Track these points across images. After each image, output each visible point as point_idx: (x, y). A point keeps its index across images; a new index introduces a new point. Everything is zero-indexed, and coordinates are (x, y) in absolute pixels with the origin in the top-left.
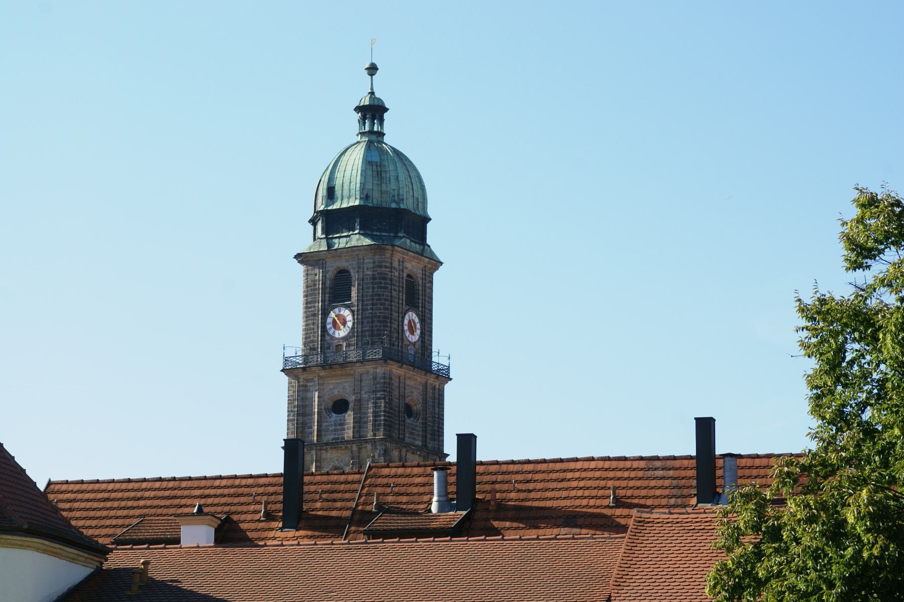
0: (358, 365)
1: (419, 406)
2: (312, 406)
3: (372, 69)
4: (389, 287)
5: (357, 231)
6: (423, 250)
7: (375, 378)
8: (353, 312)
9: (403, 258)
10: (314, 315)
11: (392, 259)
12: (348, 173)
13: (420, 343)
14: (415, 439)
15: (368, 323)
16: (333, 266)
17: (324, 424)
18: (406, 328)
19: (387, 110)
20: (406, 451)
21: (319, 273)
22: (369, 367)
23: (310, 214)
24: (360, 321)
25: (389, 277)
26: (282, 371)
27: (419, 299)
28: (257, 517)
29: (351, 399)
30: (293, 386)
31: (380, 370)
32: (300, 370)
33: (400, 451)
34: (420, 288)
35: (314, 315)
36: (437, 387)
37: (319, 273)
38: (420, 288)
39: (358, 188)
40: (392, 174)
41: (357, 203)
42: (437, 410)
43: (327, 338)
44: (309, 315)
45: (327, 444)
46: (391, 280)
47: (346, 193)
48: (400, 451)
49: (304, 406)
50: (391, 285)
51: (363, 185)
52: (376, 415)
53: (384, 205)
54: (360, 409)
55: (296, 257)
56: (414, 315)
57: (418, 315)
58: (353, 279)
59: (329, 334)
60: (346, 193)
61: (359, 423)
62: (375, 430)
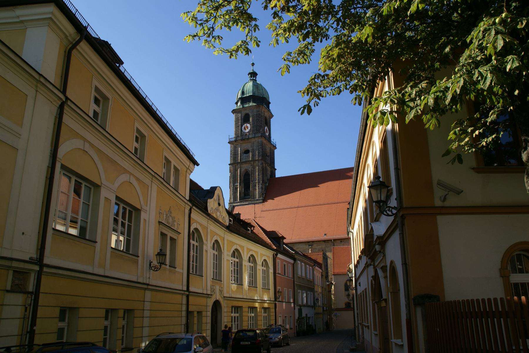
2: (238, 152)
3: (253, 64)
7: (258, 142)
8: (251, 125)
10: (238, 127)
12: (248, 88)
16: (244, 113)
17: (242, 157)
21: (240, 115)
22: (256, 139)
24: (253, 127)
26: (229, 143)
29: (250, 149)
31: (260, 140)
37: (240, 115)
39: (252, 90)
40: (261, 88)
41: (251, 94)
43: (243, 132)
44: (237, 126)
45: (243, 162)
47: (248, 92)
49: (236, 152)
51: (253, 90)
52: (259, 153)
54: (253, 152)
58: (250, 115)
60: (248, 92)
61: (253, 156)
62: (259, 156)
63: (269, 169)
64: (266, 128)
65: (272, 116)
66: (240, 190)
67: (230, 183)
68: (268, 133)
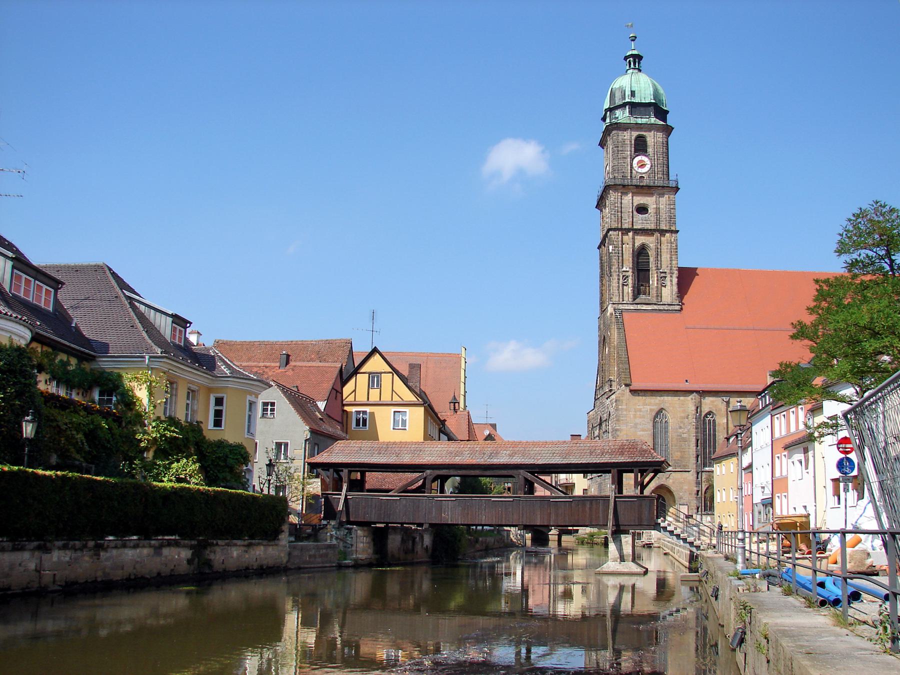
0: (660, 188)
43: (633, 171)
59: (635, 170)
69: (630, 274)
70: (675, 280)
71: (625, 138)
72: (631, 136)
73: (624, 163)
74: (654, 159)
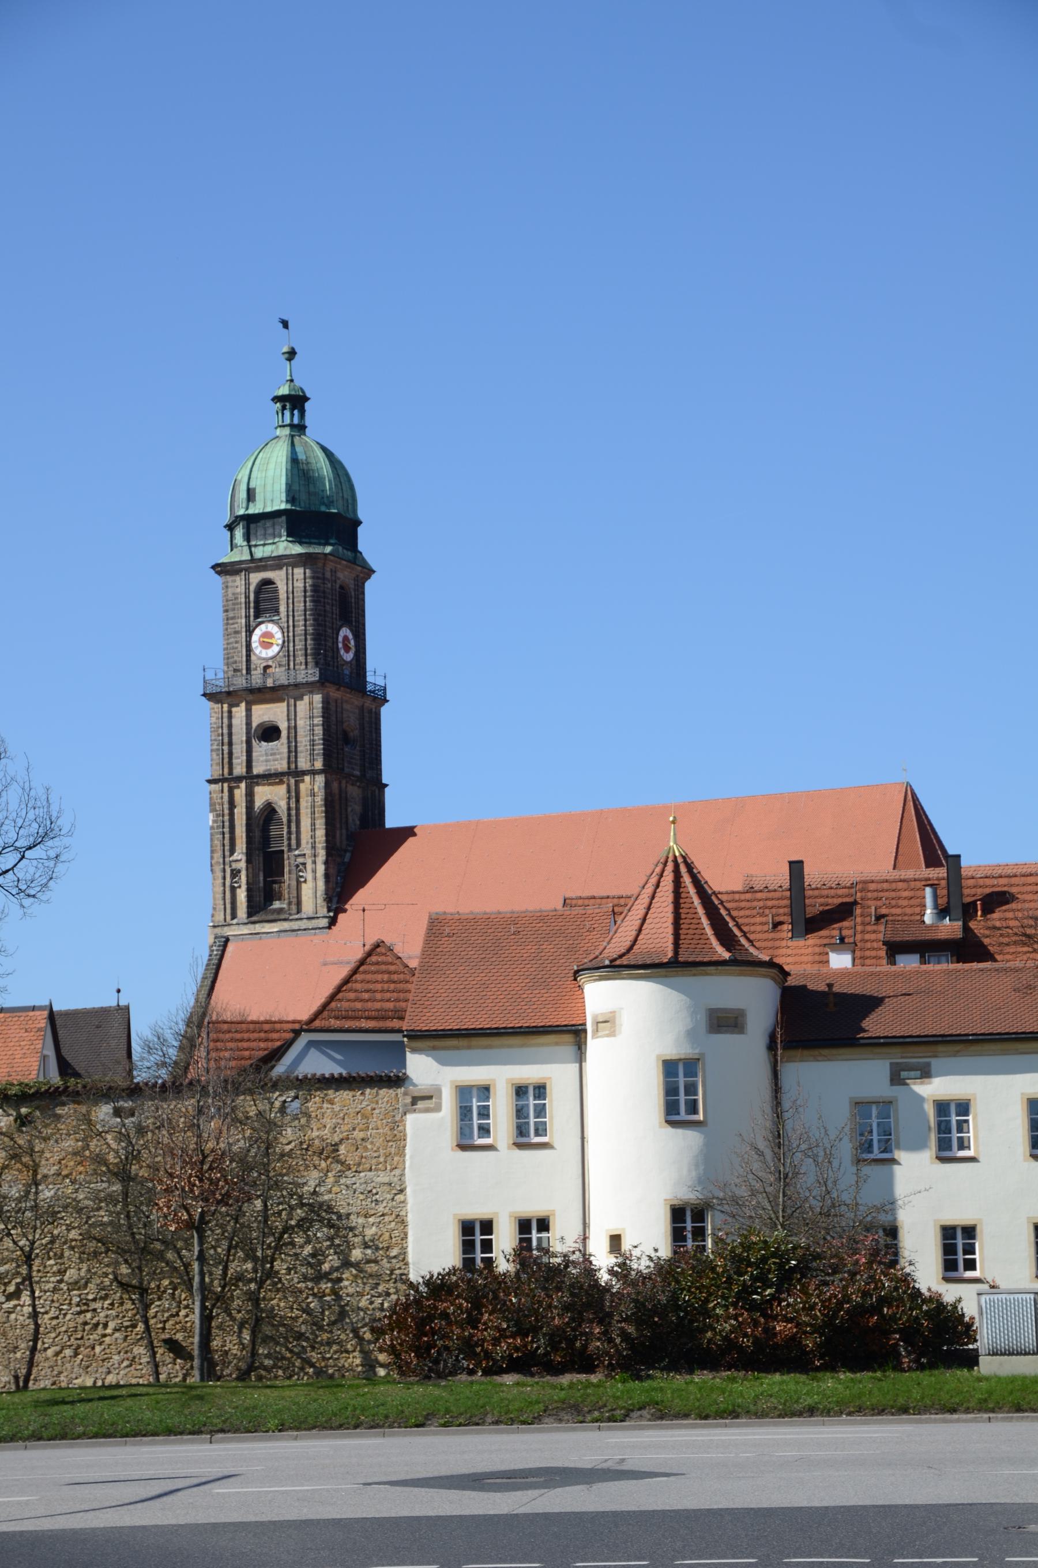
1: (357, 732)
4: (322, 600)
5: (284, 538)
6: (355, 558)
9: (336, 568)
11: (324, 569)
13: (354, 662)
14: (353, 769)
15: (300, 640)
18: (340, 645)
19: (307, 399)
20: (347, 782)
23: (227, 519)
25: (322, 589)
27: (352, 612)
28: (766, 928)
29: (283, 726)
30: (216, 713)
32: (225, 695)
33: (340, 783)
34: (353, 600)
35: (236, 632)
36: (374, 710)
38: (353, 600)
42: (374, 735)
43: (253, 658)
44: (229, 634)
45: (258, 776)
46: (324, 592)
48: (340, 783)
50: (324, 598)
52: (312, 743)
53: (313, 508)
55: (213, 567)
56: (348, 631)
57: (351, 631)
59: (255, 654)
62: (312, 760)
63: (354, 791)
64: (345, 632)
65: (369, 572)
66: (251, 881)
67: (212, 852)
68: (353, 650)
69: (242, 865)
70: (321, 868)
71: (238, 590)
72: (247, 584)
73: (237, 642)
74: (288, 627)
